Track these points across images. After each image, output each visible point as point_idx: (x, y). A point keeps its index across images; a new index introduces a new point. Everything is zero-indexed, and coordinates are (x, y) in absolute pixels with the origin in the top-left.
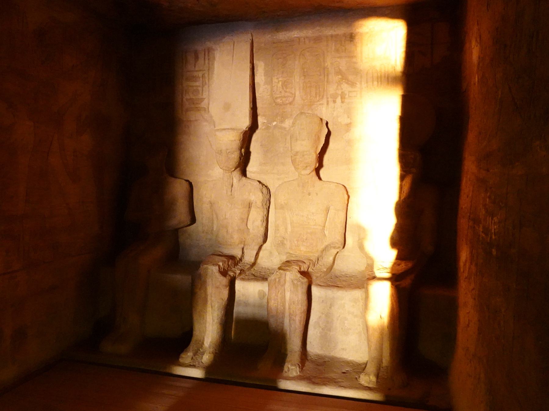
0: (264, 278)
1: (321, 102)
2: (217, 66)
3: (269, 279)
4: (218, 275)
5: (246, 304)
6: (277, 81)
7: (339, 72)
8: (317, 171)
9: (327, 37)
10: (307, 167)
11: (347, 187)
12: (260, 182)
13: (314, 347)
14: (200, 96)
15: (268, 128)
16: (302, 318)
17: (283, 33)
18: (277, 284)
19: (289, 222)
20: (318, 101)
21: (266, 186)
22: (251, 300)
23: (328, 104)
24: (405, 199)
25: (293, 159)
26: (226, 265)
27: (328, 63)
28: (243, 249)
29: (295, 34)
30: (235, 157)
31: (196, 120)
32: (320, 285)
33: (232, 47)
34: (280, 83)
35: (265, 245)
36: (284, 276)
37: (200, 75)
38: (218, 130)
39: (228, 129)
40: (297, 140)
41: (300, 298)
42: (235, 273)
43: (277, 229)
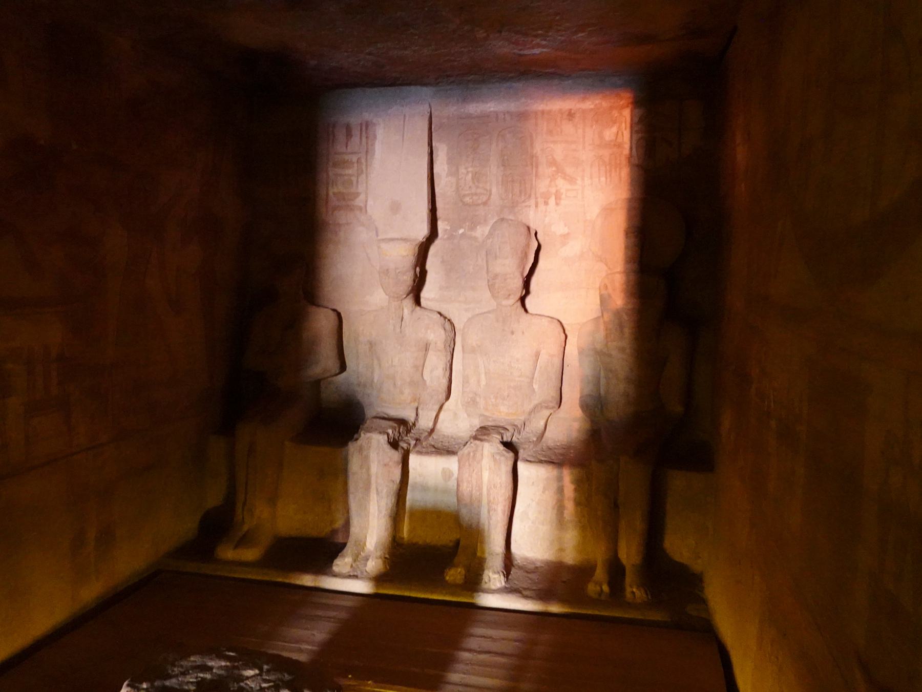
0: (447, 451)
1: (527, 204)
2: (379, 148)
4: (387, 447)
5: (425, 488)
7: (553, 163)
8: (522, 300)
9: (536, 113)
11: (563, 322)
14: (353, 190)
15: (451, 237)
17: (474, 105)
20: (524, 202)
22: (431, 482)
23: (537, 206)
26: (397, 434)
27: (537, 148)
29: (491, 106)
30: (408, 279)
33: (402, 122)
34: (470, 175)
37: (355, 159)
38: (383, 240)
39: (398, 239)
40: (496, 257)
43: (466, 381)
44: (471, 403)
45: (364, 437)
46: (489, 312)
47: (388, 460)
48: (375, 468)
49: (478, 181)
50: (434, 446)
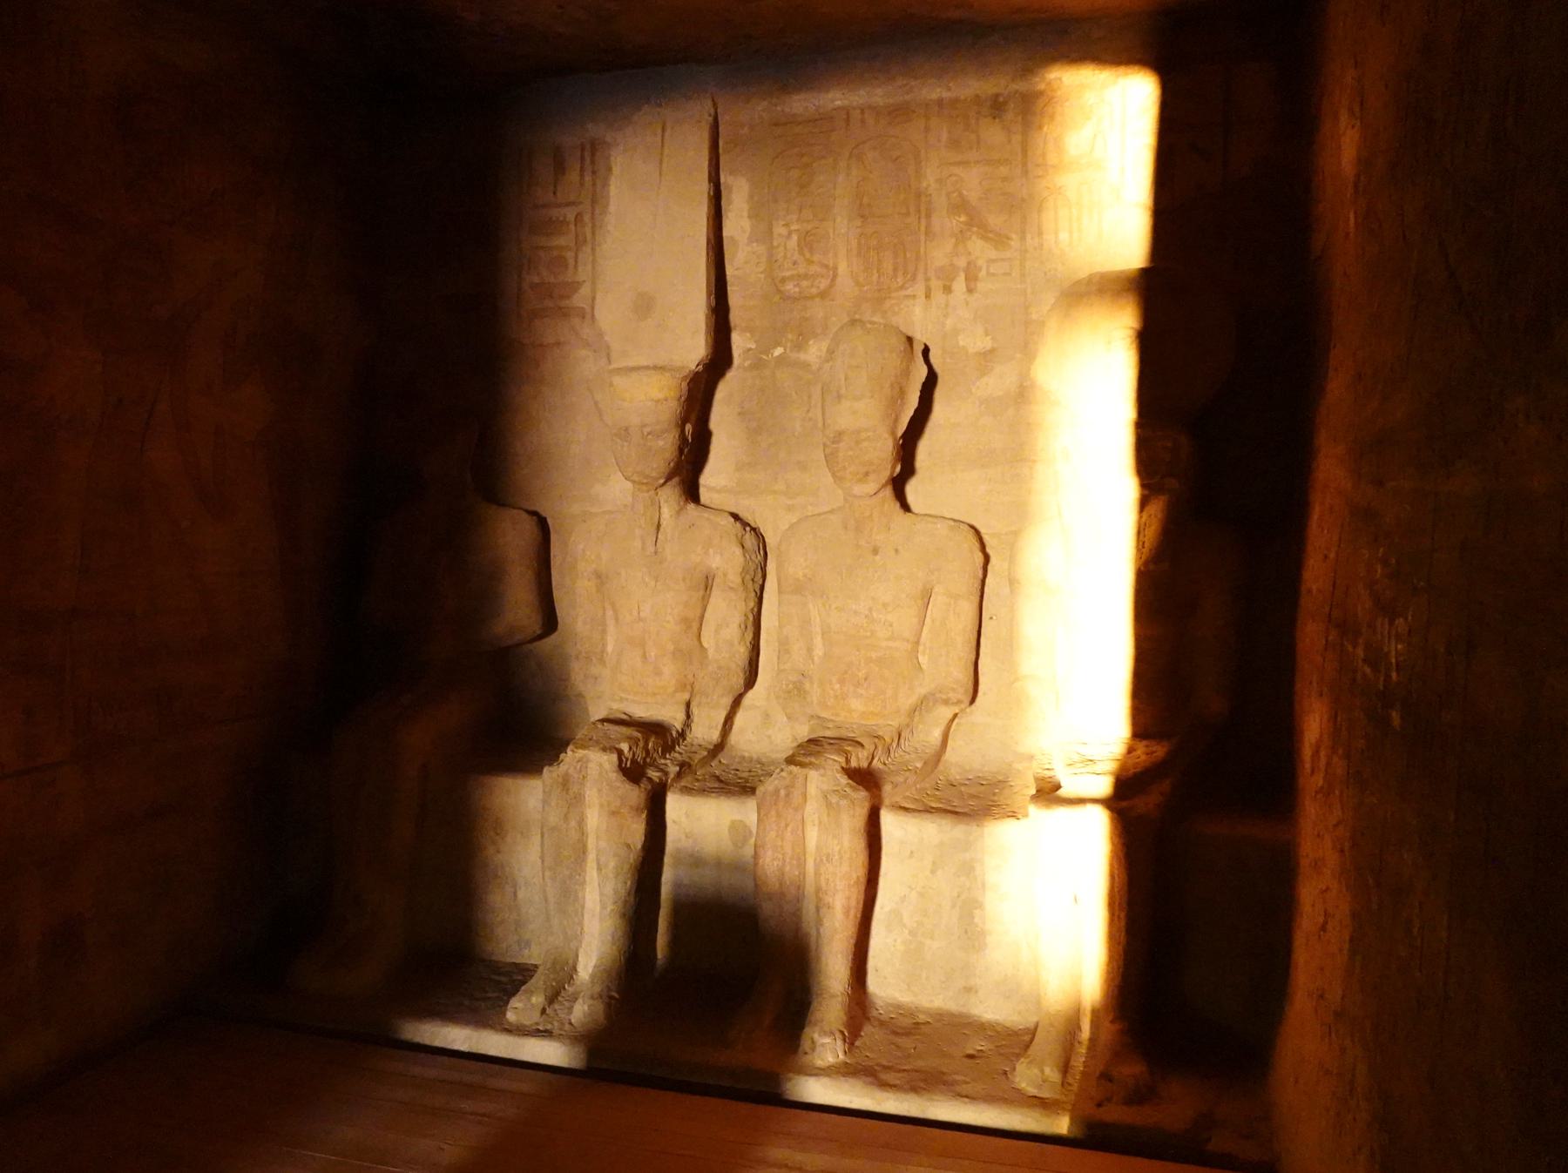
1: (909, 292)
2: (618, 192)
3: (760, 790)
6: (784, 231)
7: (960, 205)
8: (898, 486)
10: (867, 474)
11: (983, 531)
12: (736, 517)
13: (887, 983)
15: (758, 365)
16: (853, 903)
17: (802, 96)
18: (781, 804)
19: (818, 629)
20: (902, 288)
21: (754, 529)
23: (928, 296)
24: (1146, 563)
25: (828, 451)
27: (930, 178)
28: (688, 705)
29: (836, 98)
30: (666, 446)
31: (558, 344)
32: (906, 809)
33: (659, 139)
34: (795, 237)
35: (750, 694)
36: (801, 780)
37: (571, 217)
38: (619, 371)
39: (647, 368)
40: (839, 397)
41: (846, 844)
42: (666, 774)
43: (784, 648)
44: (795, 691)
45: (570, 756)
46: (832, 511)
47: (618, 803)
48: (594, 819)
49: (811, 250)
50: (718, 779)
